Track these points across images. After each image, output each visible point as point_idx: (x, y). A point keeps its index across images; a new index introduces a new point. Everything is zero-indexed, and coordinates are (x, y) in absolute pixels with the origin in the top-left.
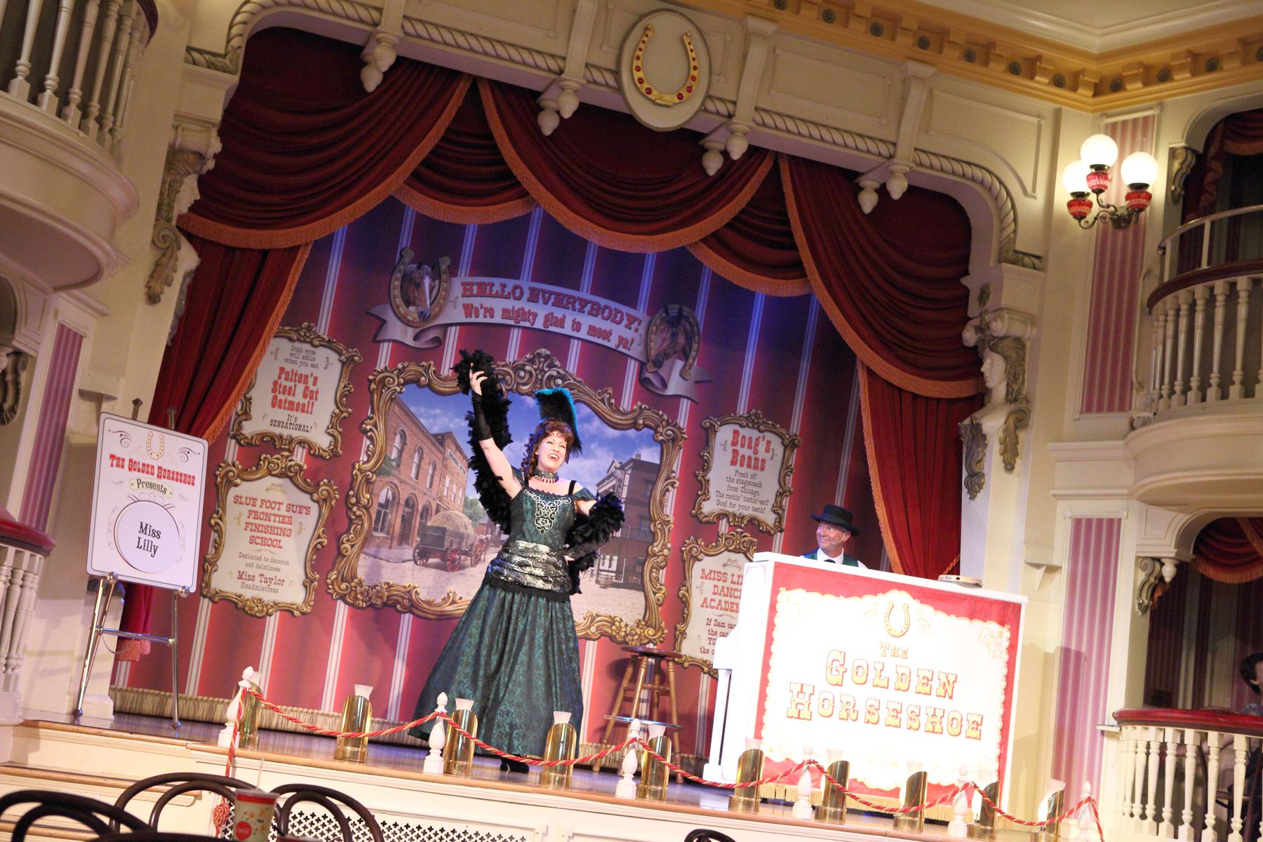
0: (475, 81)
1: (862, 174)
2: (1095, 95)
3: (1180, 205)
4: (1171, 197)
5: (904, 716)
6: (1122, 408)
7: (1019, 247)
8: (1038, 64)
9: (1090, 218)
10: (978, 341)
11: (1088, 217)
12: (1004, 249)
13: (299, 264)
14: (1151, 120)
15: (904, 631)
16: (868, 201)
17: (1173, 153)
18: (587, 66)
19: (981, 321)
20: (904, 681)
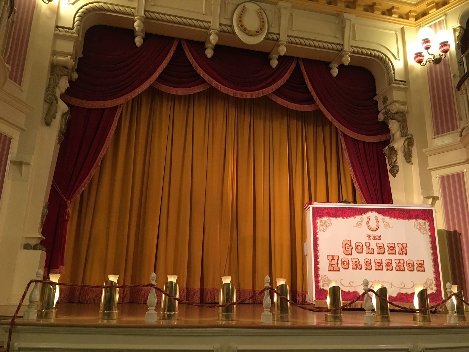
0: (180, 40)
1: (331, 62)
2: (416, 20)
3: (460, 50)
4: (458, 47)
5: (384, 265)
6: (453, 129)
7: (397, 78)
8: (393, 10)
9: (424, 62)
10: (384, 119)
11: (423, 61)
12: (390, 80)
13: (118, 114)
14: (442, 21)
15: (377, 228)
16: (335, 72)
17: (455, 30)
18: (220, 24)
19: (385, 109)
20: (381, 249)
